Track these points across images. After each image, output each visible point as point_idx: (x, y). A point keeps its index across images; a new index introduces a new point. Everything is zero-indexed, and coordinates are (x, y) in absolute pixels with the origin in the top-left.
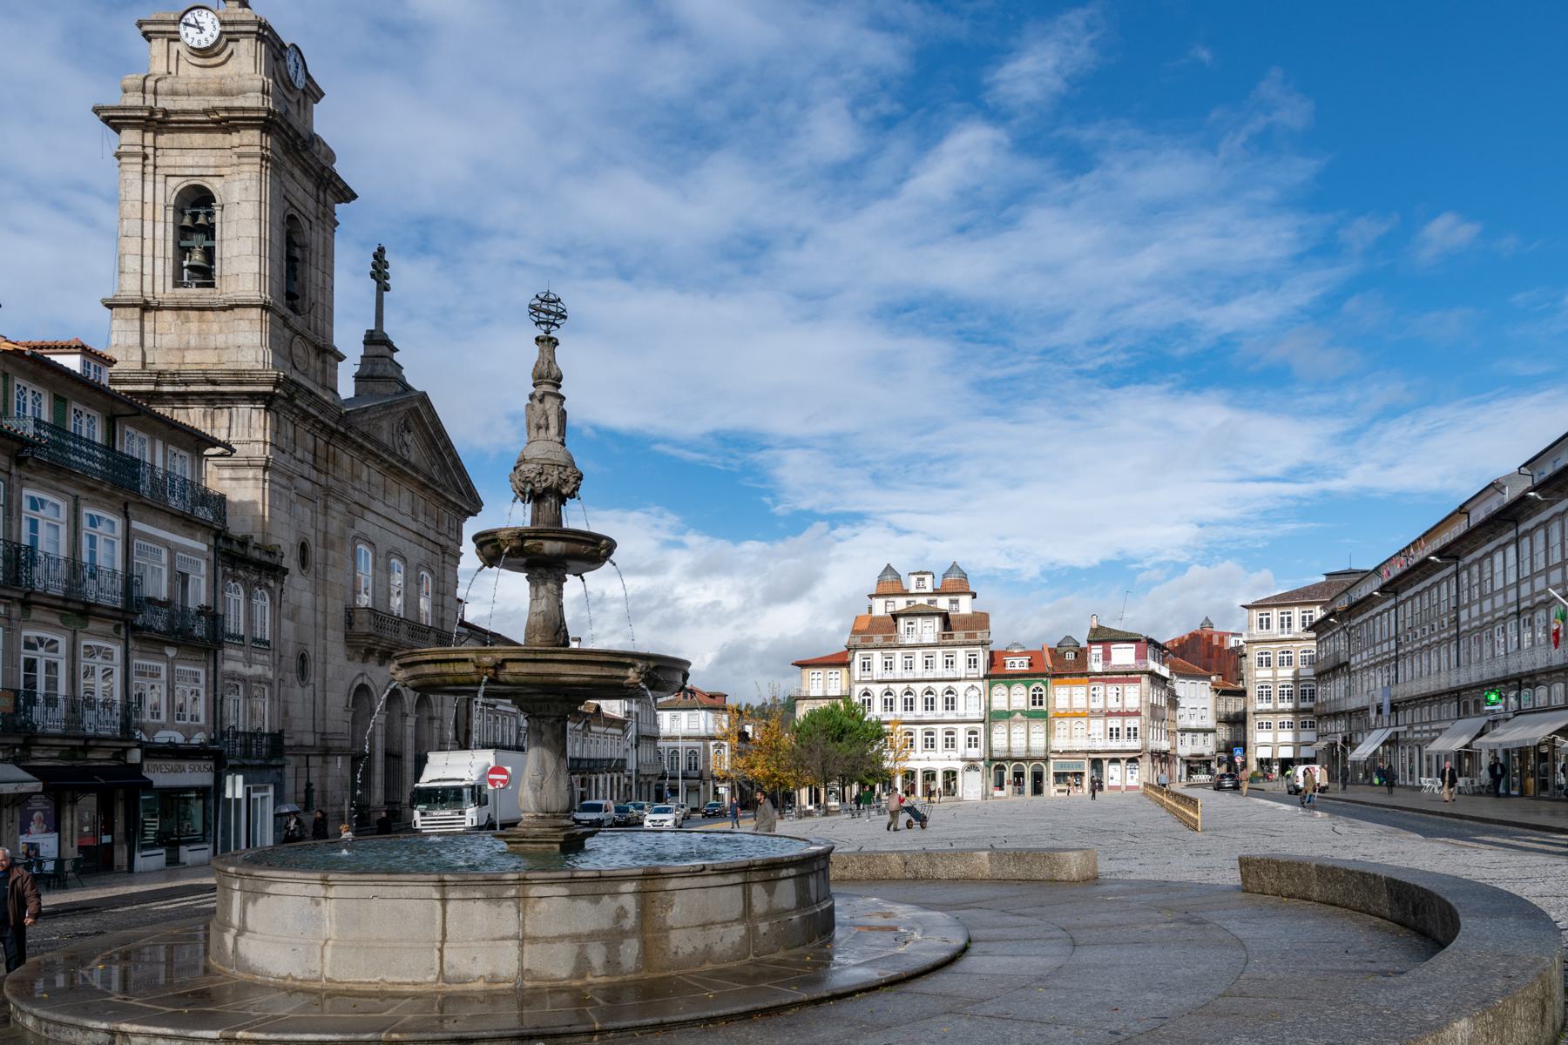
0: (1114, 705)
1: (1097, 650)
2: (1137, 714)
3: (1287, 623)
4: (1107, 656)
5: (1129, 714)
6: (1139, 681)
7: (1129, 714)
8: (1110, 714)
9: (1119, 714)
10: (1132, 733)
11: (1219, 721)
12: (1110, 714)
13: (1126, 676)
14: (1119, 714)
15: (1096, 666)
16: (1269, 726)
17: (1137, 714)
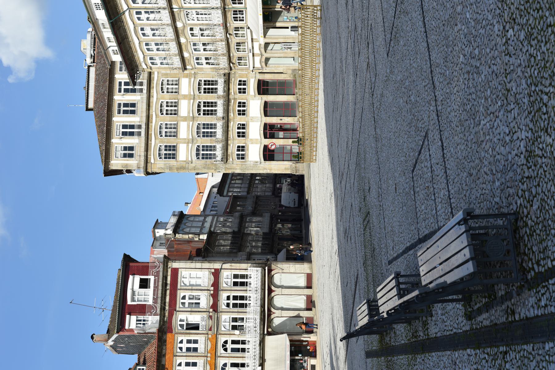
0: (205, 301)
1: (131, 322)
2: (216, 274)
3: (129, 130)
4: (141, 309)
5: (216, 285)
6: (175, 272)
7: (216, 285)
8: (215, 307)
9: (215, 296)
10: (240, 282)
11: (240, 250)
12: (215, 307)
13: (170, 287)
14: (215, 296)
15: (152, 321)
16: (241, 148)
17: (216, 274)
